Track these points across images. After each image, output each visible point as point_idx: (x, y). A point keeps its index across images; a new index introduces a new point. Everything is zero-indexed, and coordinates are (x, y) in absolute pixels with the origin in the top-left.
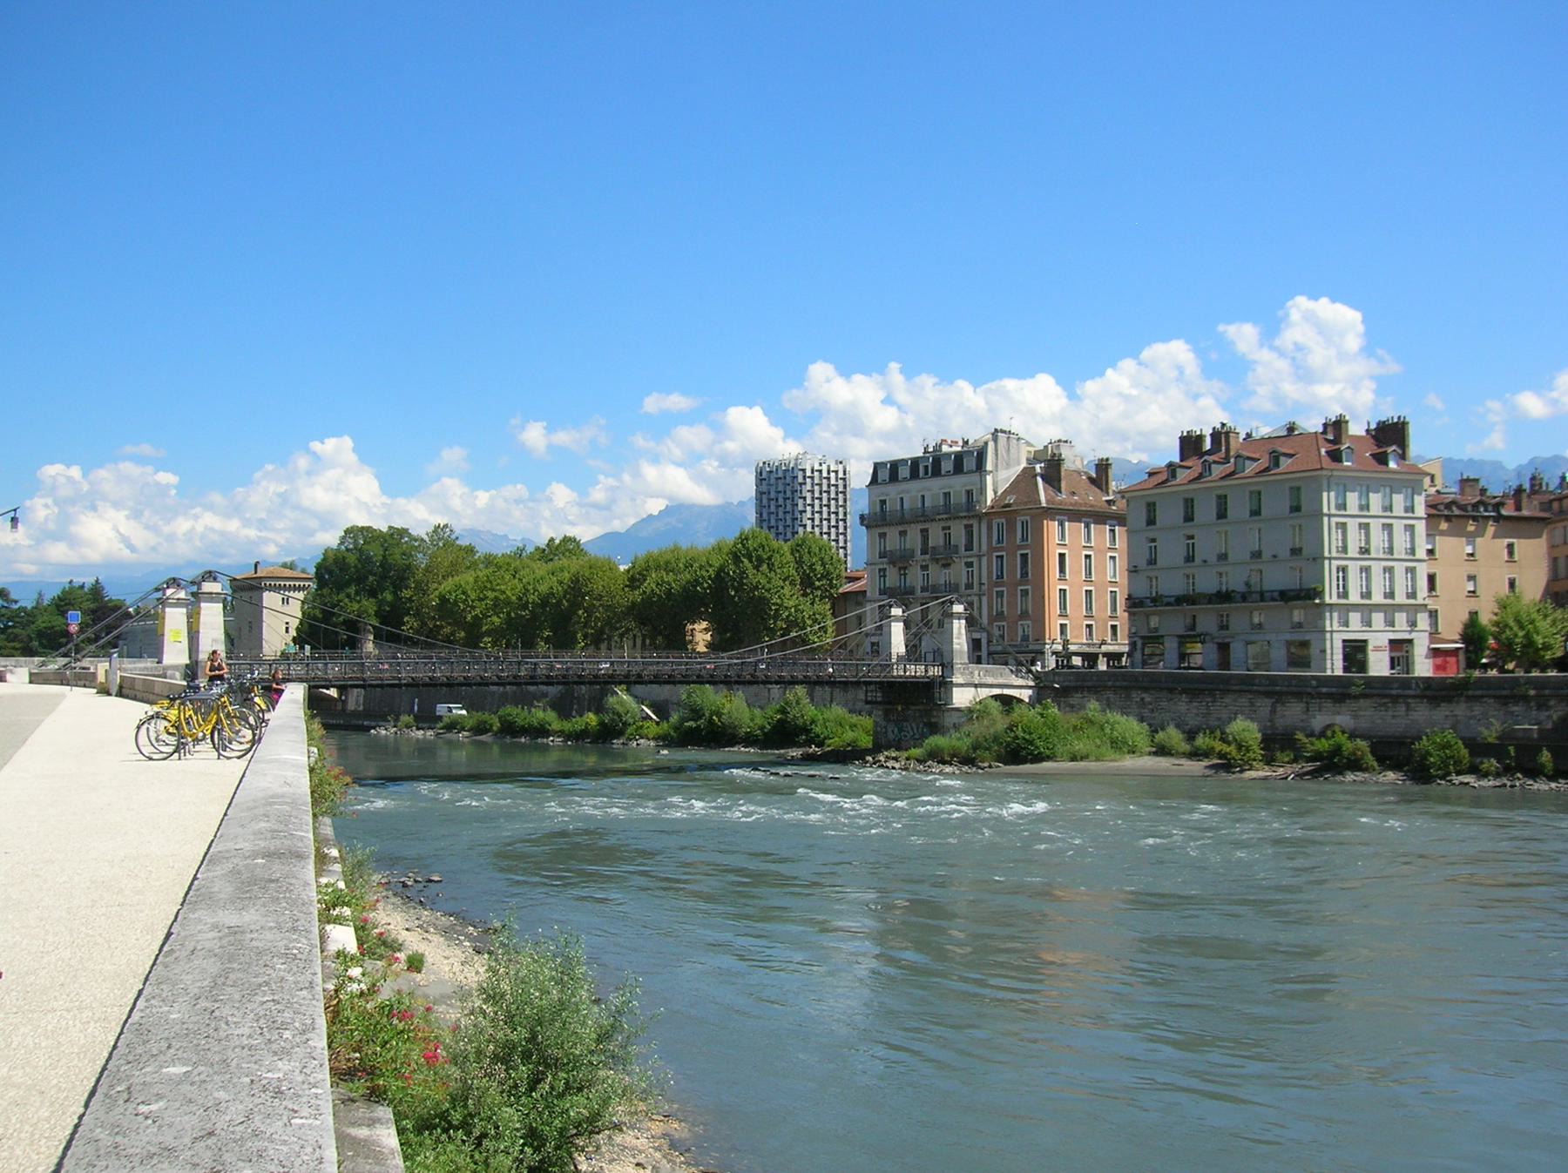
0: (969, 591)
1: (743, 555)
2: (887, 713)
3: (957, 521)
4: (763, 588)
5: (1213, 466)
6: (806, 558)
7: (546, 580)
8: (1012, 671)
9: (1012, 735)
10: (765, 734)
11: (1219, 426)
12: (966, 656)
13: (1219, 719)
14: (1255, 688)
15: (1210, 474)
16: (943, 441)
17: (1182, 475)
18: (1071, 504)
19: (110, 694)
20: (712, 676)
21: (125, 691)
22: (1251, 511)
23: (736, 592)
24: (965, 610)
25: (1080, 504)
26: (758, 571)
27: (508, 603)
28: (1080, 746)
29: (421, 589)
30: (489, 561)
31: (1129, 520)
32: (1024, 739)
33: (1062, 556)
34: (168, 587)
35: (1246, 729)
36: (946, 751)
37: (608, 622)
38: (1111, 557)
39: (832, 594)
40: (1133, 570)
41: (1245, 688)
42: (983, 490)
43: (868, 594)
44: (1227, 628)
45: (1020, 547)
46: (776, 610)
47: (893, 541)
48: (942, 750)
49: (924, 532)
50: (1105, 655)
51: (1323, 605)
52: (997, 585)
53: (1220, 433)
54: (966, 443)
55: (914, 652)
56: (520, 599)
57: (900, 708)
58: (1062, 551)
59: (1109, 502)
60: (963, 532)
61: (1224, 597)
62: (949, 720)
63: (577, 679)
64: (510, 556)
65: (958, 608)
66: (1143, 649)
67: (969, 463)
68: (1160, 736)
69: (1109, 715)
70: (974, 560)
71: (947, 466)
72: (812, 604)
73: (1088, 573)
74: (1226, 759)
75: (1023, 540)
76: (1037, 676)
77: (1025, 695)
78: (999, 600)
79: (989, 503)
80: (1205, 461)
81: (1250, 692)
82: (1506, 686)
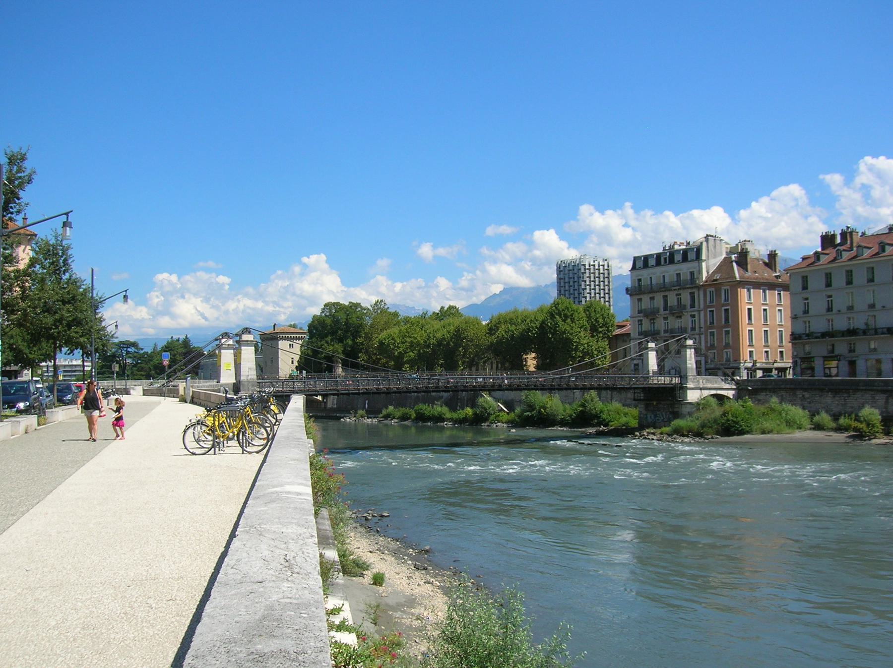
1: (556, 314)
2: (647, 407)
3: (685, 290)
4: (568, 333)
5: (843, 252)
6: (593, 314)
7: (441, 331)
8: (722, 379)
9: (725, 418)
10: (572, 419)
11: (845, 228)
12: (695, 371)
13: (852, 407)
14: (875, 388)
15: (841, 258)
16: (675, 243)
17: (824, 259)
18: (754, 279)
19: (186, 402)
20: (543, 385)
21: (195, 400)
22: (868, 279)
23: (552, 336)
24: (694, 343)
25: (760, 279)
26: (565, 322)
27: (418, 344)
28: (767, 425)
29: (368, 338)
30: (407, 320)
31: (791, 287)
32: (733, 421)
33: (749, 310)
34: (222, 338)
35: (871, 413)
36: (684, 429)
37: (477, 355)
38: (779, 310)
39: (609, 336)
40: (794, 318)
41: (870, 388)
43: (632, 335)
44: (854, 351)
45: (724, 305)
46: (577, 346)
47: (646, 303)
48: (682, 428)
49: (665, 297)
50: (776, 369)
52: (711, 328)
53: (847, 233)
54: (688, 244)
55: (661, 371)
56: (425, 342)
57: (655, 403)
58: (750, 307)
59: (776, 277)
60: (689, 297)
61: (852, 332)
62: (685, 410)
63: (463, 388)
64: (418, 318)
65: (690, 342)
66: (801, 365)
67: (692, 255)
68: (816, 418)
69: (784, 406)
70: (696, 313)
71: (678, 257)
72: (597, 342)
73: (766, 320)
74: (860, 432)
76: (737, 383)
77: (730, 394)
78: (712, 337)
79: (704, 279)
80: (838, 250)
81: (872, 390)
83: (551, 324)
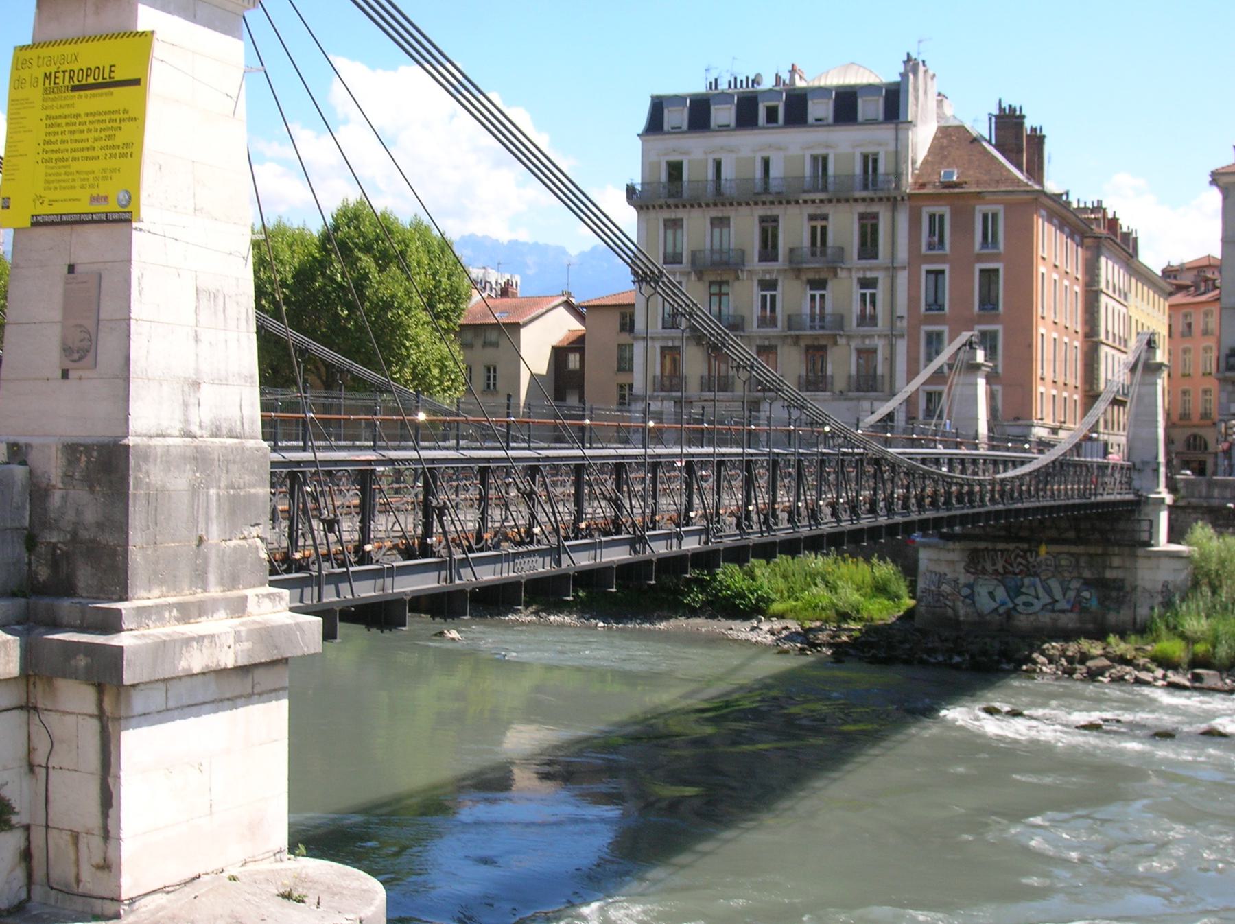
0: (866, 330)
3: (843, 207)
42: (898, 156)
45: (980, 258)
52: (928, 320)
67: (869, 108)
71: (820, 109)
83: (343, 275)
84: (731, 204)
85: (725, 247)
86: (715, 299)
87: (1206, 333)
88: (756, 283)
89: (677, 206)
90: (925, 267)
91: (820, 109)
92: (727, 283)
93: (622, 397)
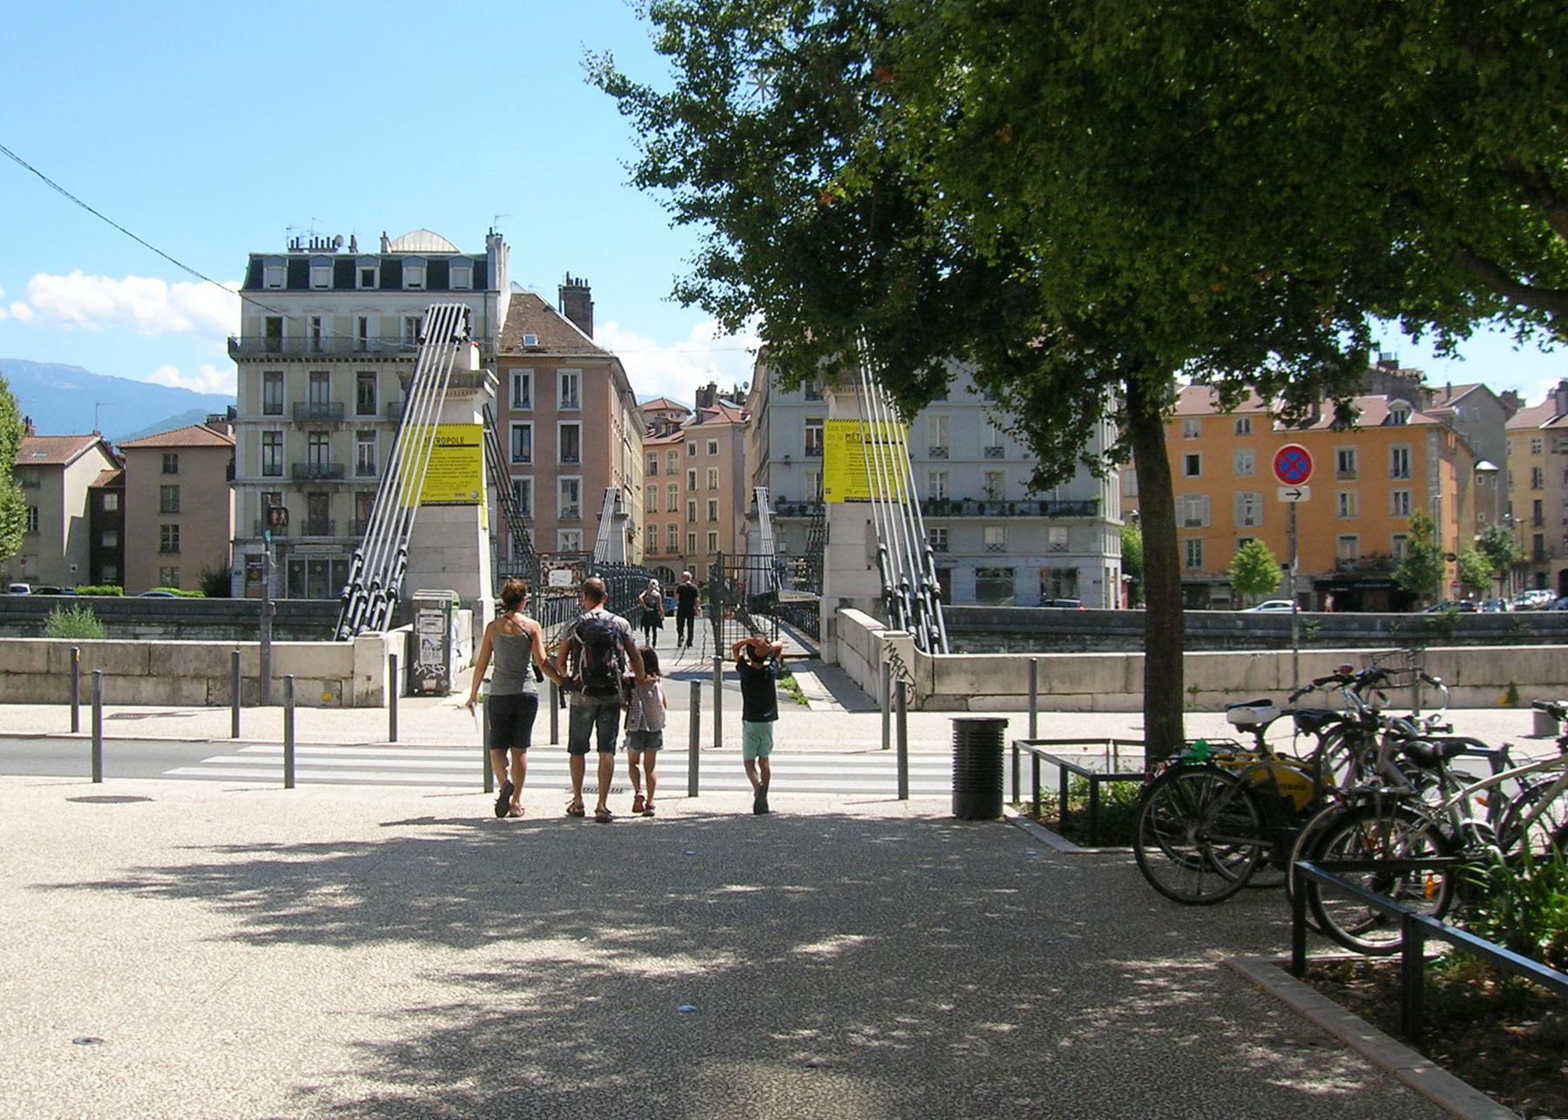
45: (561, 415)
47: (296, 383)
51: (1103, 522)
67: (460, 276)
71: (414, 275)
75: (565, 404)
82: (1494, 626)
84: (331, 360)
85: (324, 400)
86: (314, 448)
87: (670, 472)
88: (354, 434)
89: (277, 360)
90: (512, 423)
91: (414, 275)
92: (326, 433)
93: (165, 539)
